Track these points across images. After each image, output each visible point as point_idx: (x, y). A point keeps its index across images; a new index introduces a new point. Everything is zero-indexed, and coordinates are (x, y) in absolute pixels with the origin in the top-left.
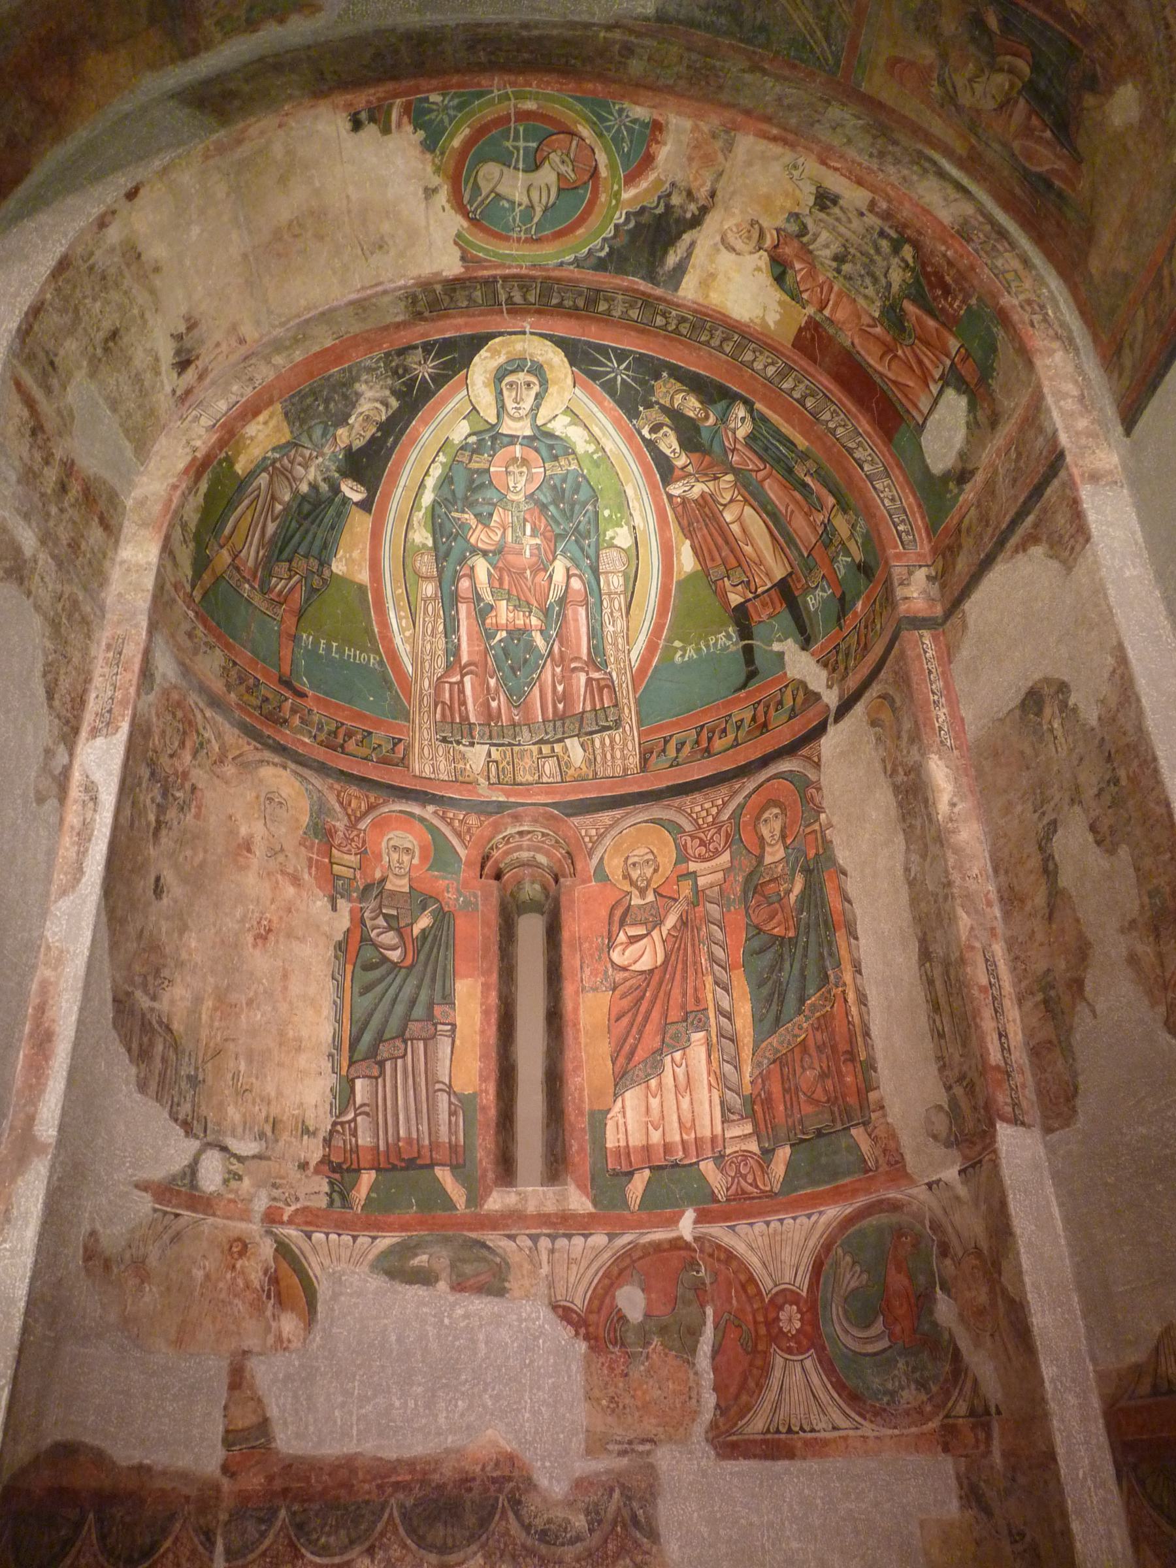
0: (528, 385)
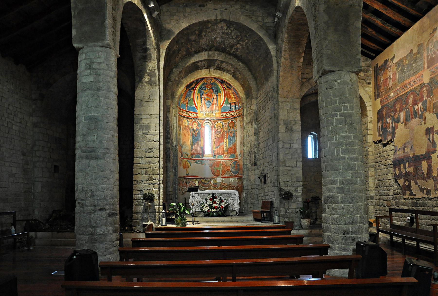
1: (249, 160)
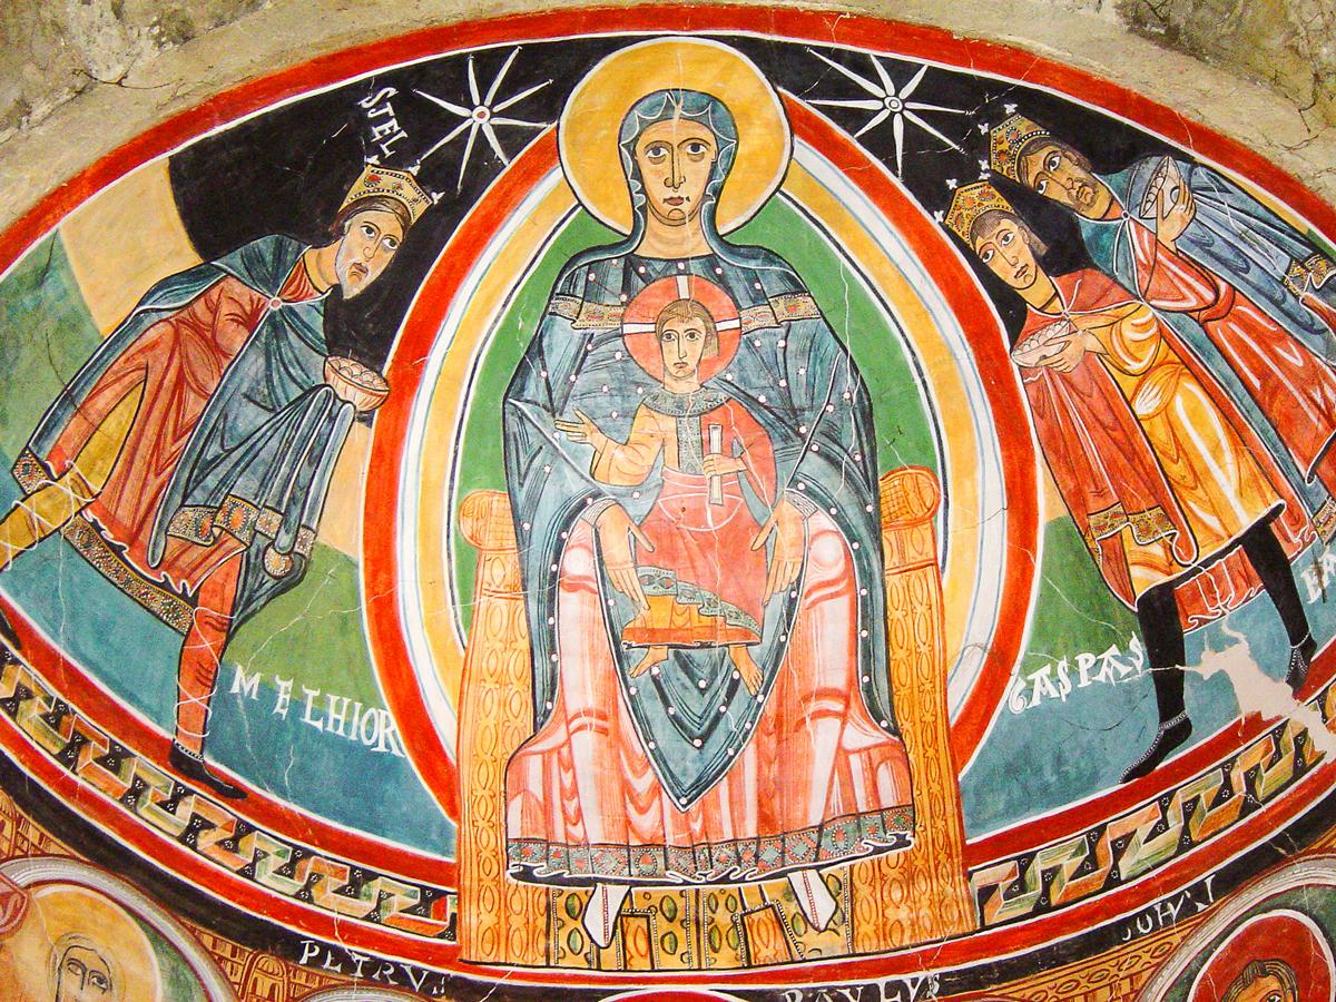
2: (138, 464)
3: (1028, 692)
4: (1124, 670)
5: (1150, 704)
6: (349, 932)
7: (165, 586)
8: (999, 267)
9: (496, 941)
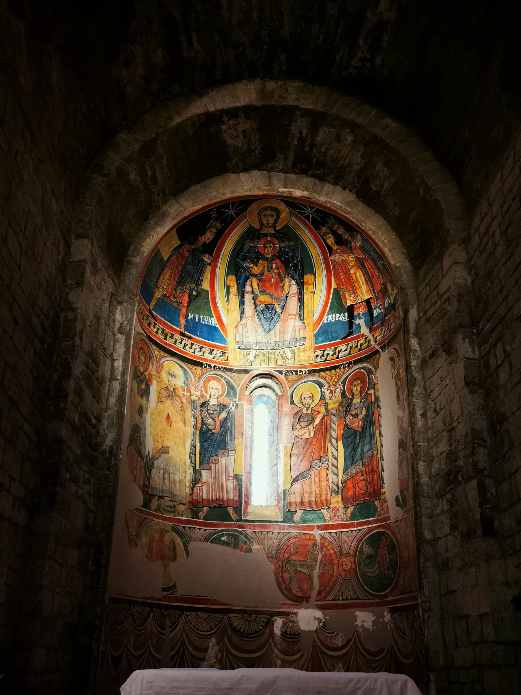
0: (272, 215)
1: (445, 518)
2: (171, 281)
3: (327, 319)
4: (344, 318)
5: (347, 326)
6: (210, 361)
7: (177, 301)
8: (328, 242)
9: (234, 361)
